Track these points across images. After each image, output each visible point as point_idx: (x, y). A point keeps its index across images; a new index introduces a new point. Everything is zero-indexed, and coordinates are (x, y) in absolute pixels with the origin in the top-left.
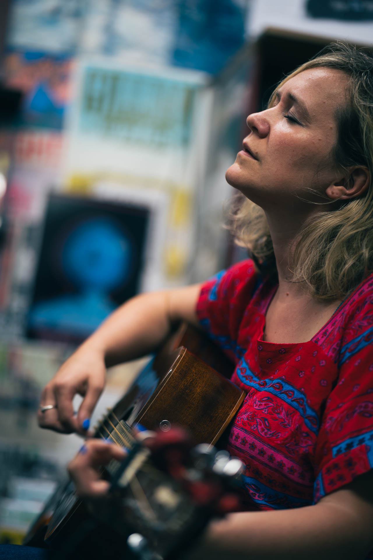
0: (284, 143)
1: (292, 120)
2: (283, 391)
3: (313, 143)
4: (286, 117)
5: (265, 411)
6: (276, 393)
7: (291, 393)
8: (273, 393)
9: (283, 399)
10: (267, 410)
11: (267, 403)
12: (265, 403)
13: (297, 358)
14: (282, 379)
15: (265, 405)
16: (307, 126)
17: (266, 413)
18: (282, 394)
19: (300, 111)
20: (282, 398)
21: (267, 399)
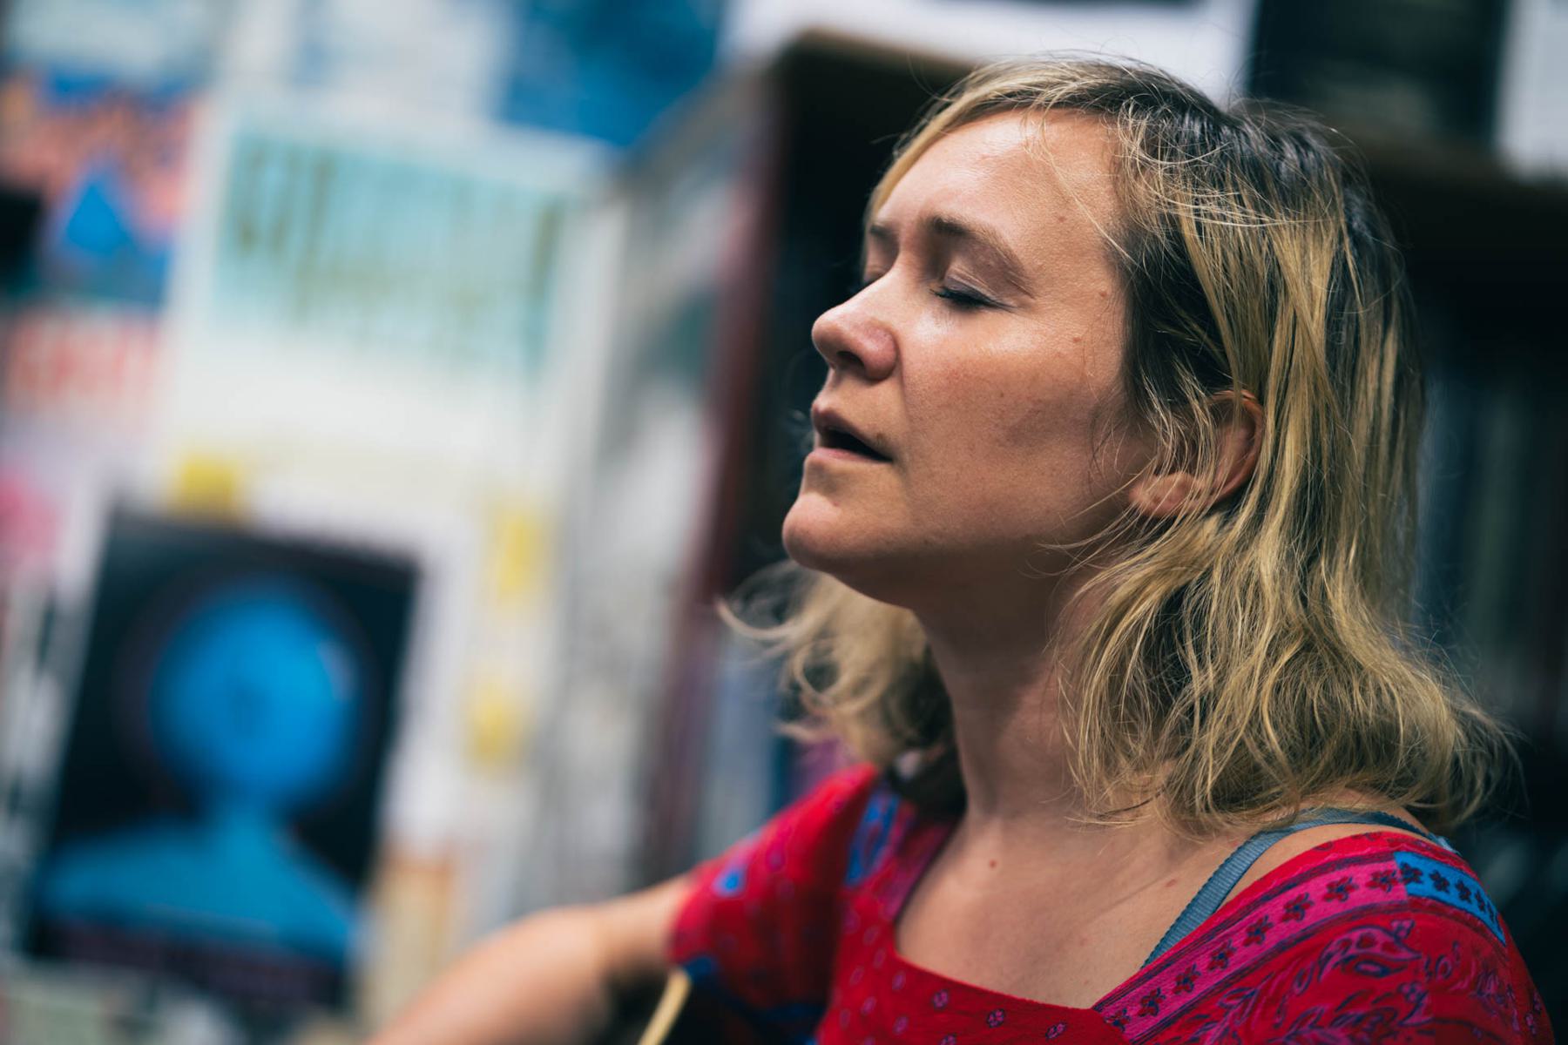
16: (1024, 307)
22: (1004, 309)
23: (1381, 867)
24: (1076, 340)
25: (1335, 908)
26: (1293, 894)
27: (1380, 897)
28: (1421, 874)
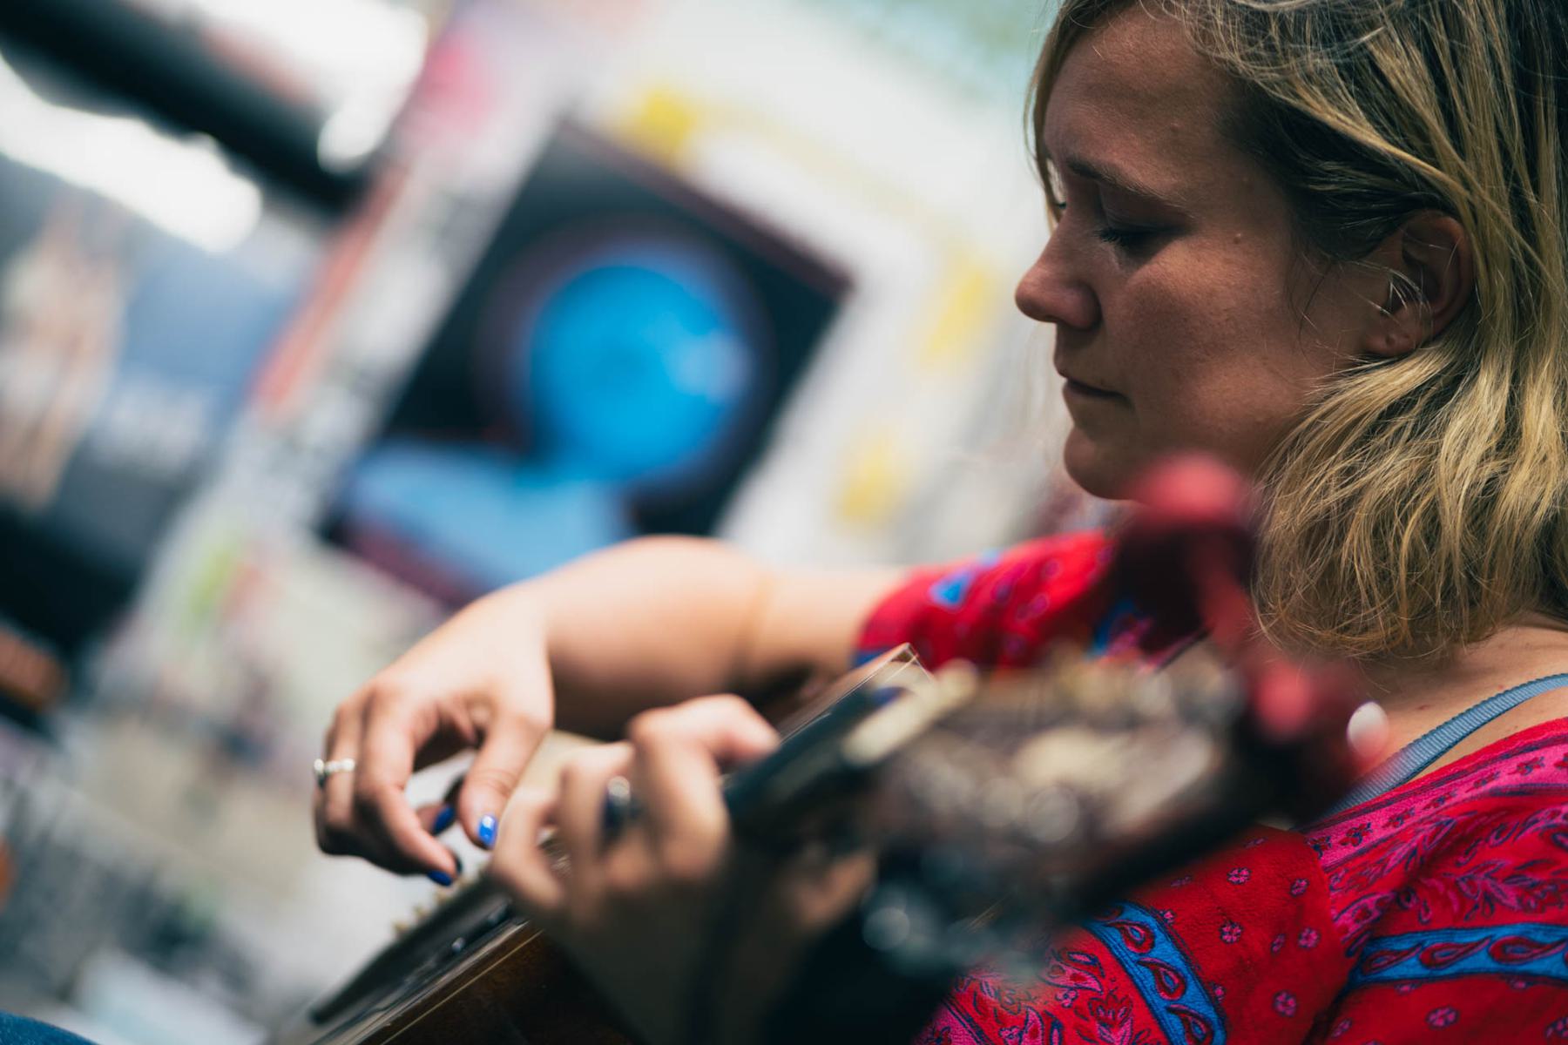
2: (1149, 960)
5: (1066, 996)
6: (1124, 954)
7: (1171, 978)
8: (1115, 952)
9: (1140, 984)
10: (1072, 995)
11: (1083, 974)
12: (1078, 972)
14: (1162, 923)
15: (1074, 977)
17: (1067, 1005)
18: (1142, 968)
20: (1137, 980)
21: (1087, 960)
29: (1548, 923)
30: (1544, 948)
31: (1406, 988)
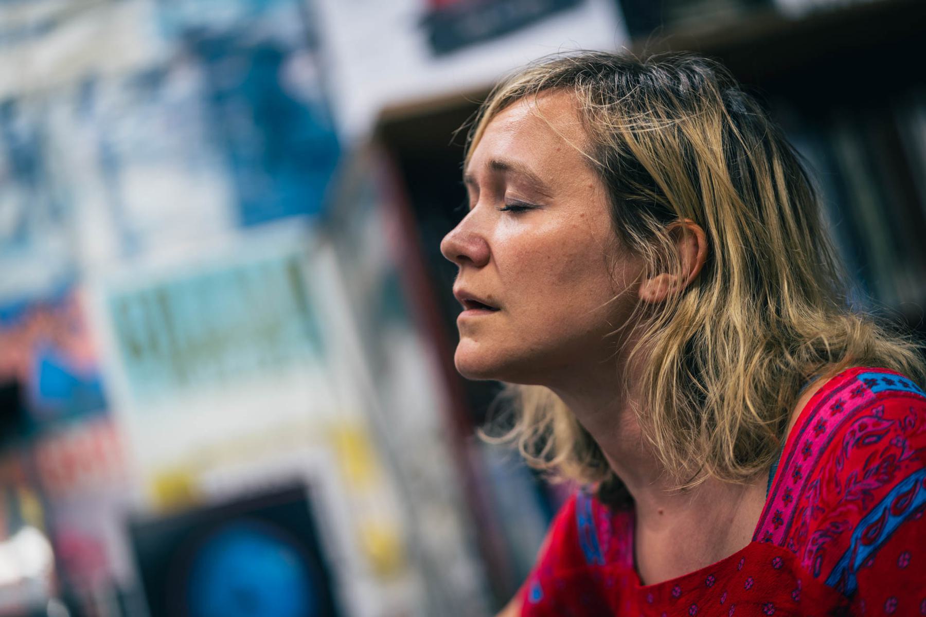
0: (526, 252)
1: (517, 210)
3: (574, 226)
4: (504, 210)
13: (747, 583)
19: (525, 183)
22: (538, 208)
23: (853, 386)
24: (582, 216)
25: (839, 417)
26: (815, 420)
27: (859, 401)
28: (877, 380)
29: (902, 481)
30: (912, 491)
31: (870, 562)
